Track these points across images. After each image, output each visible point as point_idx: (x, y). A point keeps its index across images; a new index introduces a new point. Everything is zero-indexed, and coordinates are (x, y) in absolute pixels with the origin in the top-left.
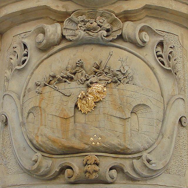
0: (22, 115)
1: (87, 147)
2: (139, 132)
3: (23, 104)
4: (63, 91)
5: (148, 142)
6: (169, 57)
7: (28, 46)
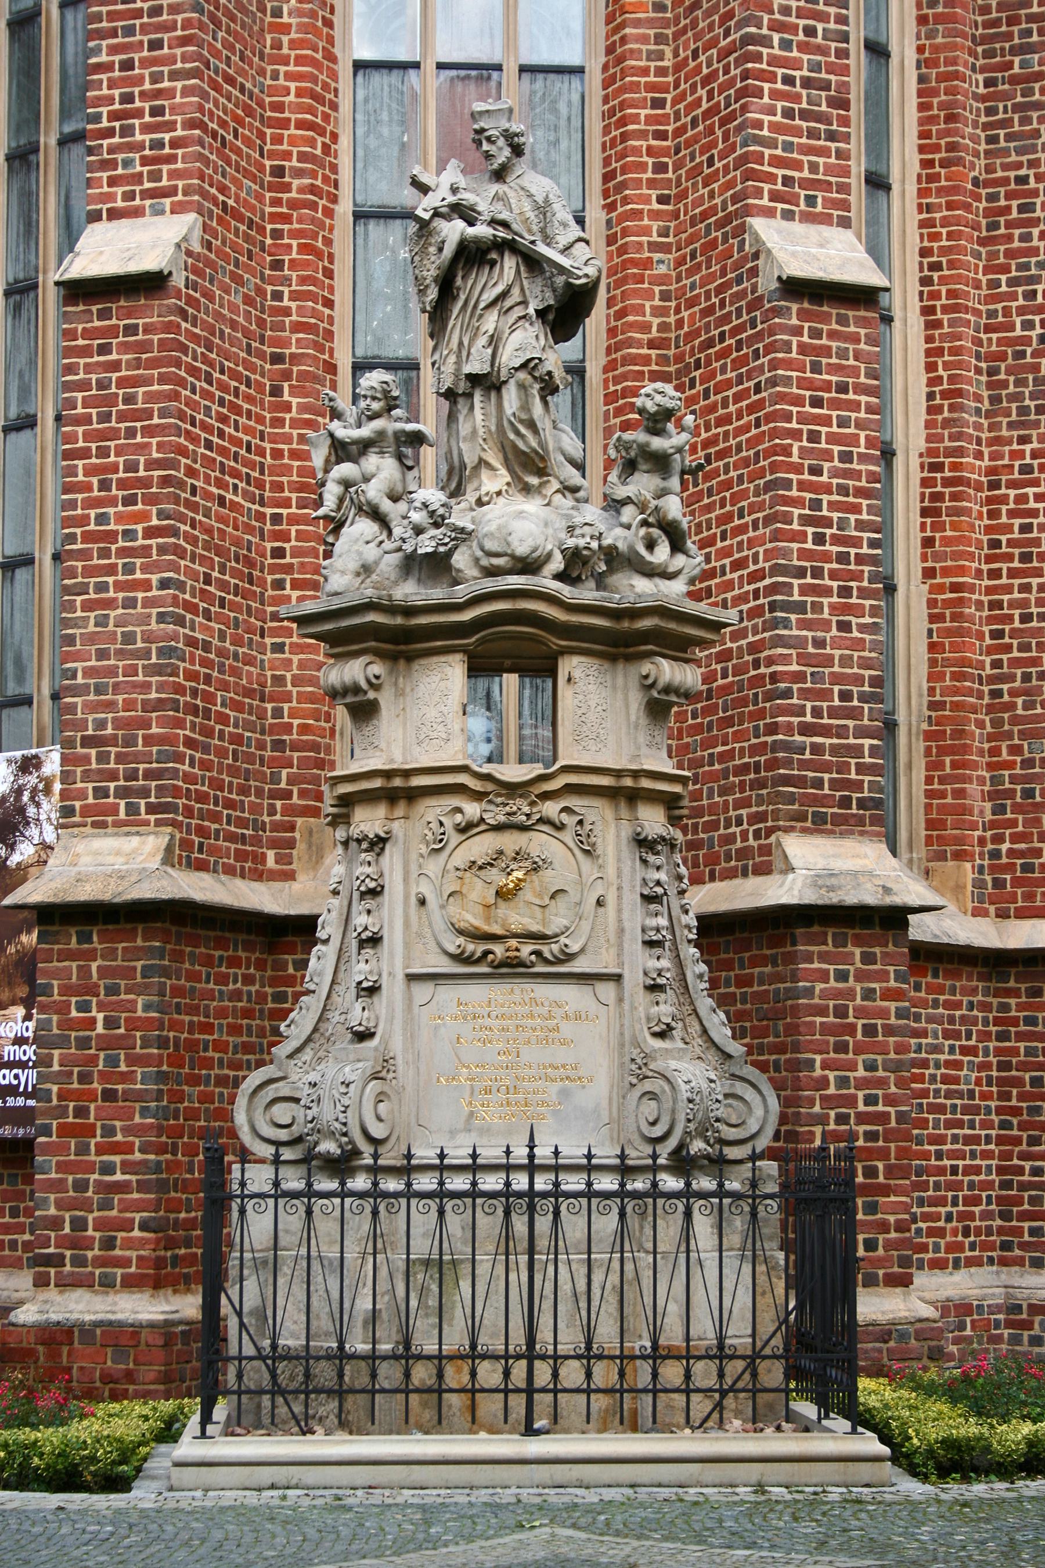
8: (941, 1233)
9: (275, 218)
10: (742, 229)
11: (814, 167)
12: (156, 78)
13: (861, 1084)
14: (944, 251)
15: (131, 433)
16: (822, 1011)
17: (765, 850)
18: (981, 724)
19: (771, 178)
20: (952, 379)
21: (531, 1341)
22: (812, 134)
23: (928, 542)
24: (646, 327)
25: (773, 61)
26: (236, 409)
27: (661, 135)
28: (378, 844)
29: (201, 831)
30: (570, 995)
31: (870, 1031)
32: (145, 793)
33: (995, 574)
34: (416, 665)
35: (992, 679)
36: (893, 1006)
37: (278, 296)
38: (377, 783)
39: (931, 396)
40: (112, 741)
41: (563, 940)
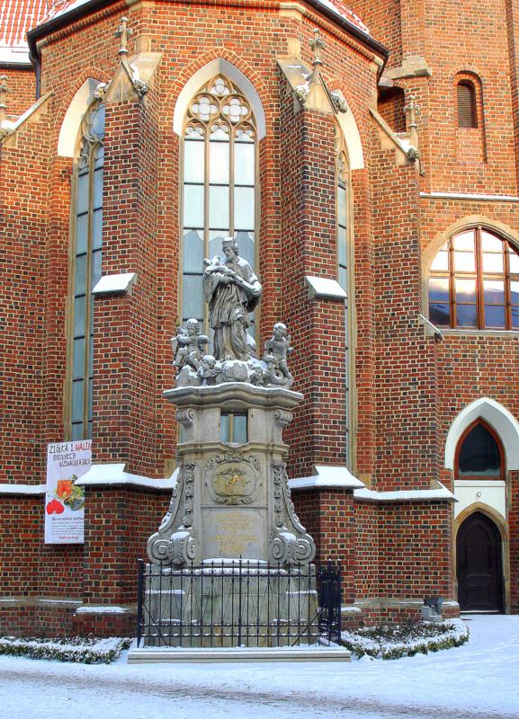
2: (248, 489)
8: (361, 587)
9: (159, 275)
10: (303, 280)
11: (325, 261)
12: (123, 232)
13: (339, 541)
14: (363, 288)
15: (115, 340)
16: (327, 519)
17: (310, 469)
18: (374, 431)
19: (312, 264)
20: (365, 326)
21: (240, 620)
22: (324, 251)
23: (358, 376)
24: (273, 309)
25: (313, 229)
26: (147, 333)
27: (278, 251)
28: (192, 467)
29: (136, 463)
30: (251, 514)
31: (342, 525)
32: (118, 450)
33: (378, 386)
34: (205, 411)
35: (377, 418)
36: (348, 517)
37: (160, 299)
38: (192, 448)
39: (359, 331)
40: (108, 434)
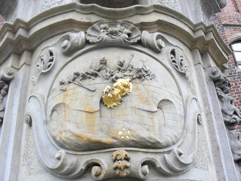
0: (46, 114)
1: (115, 141)
3: (47, 103)
4: (88, 87)
5: (176, 137)
6: (181, 64)
7: (54, 54)
41: (175, 148)
